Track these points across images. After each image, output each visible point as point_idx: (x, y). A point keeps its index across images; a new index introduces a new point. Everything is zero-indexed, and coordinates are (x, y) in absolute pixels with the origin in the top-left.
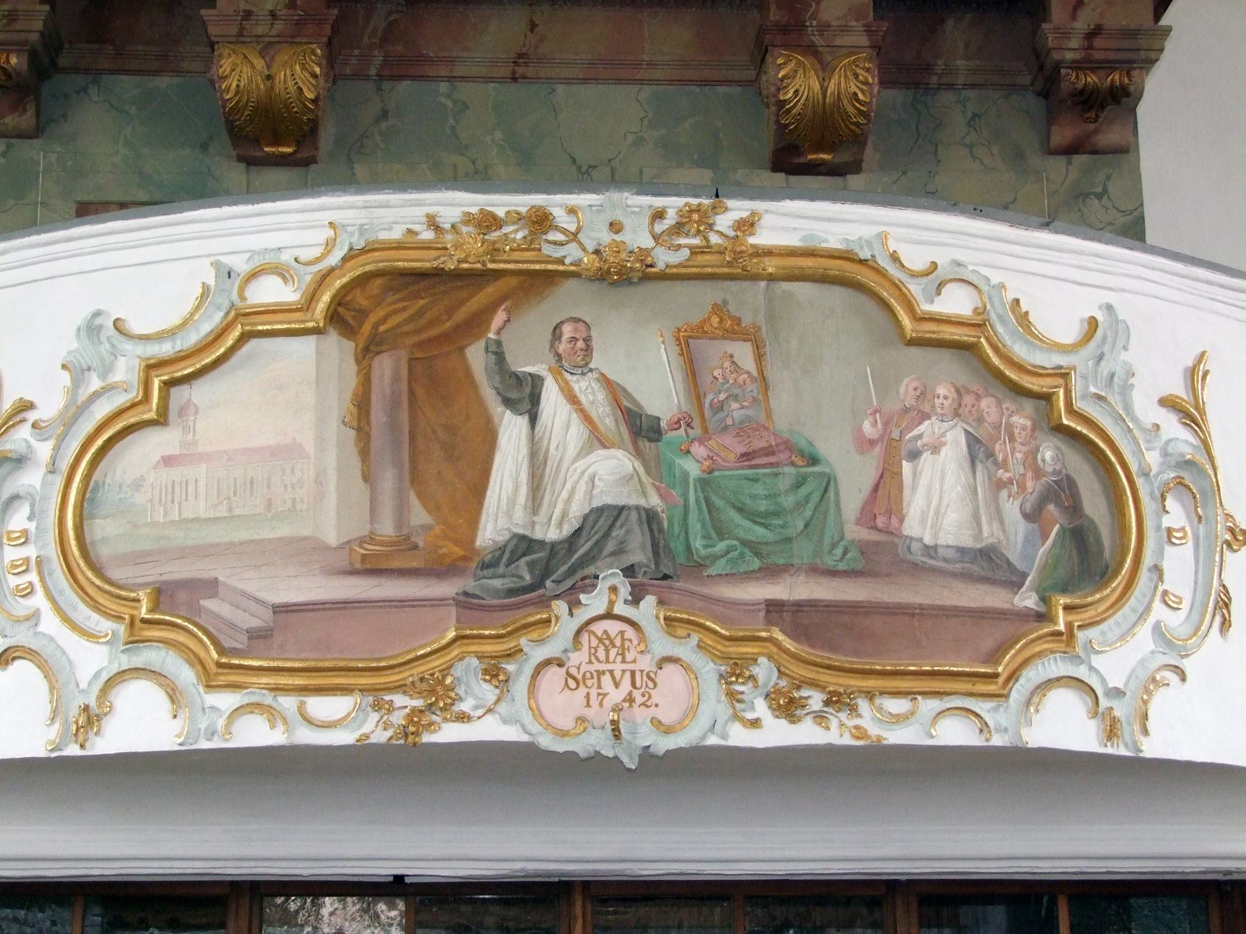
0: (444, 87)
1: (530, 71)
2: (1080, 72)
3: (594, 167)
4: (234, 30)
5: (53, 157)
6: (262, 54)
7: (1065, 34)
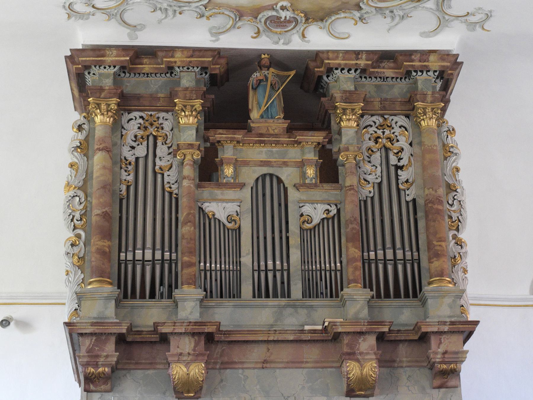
0: (240, 371)
1: (268, 365)
2: (441, 365)
3: (289, 397)
4: (176, 359)
5: (116, 398)
6: (186, 366)
7: (436, 353)
